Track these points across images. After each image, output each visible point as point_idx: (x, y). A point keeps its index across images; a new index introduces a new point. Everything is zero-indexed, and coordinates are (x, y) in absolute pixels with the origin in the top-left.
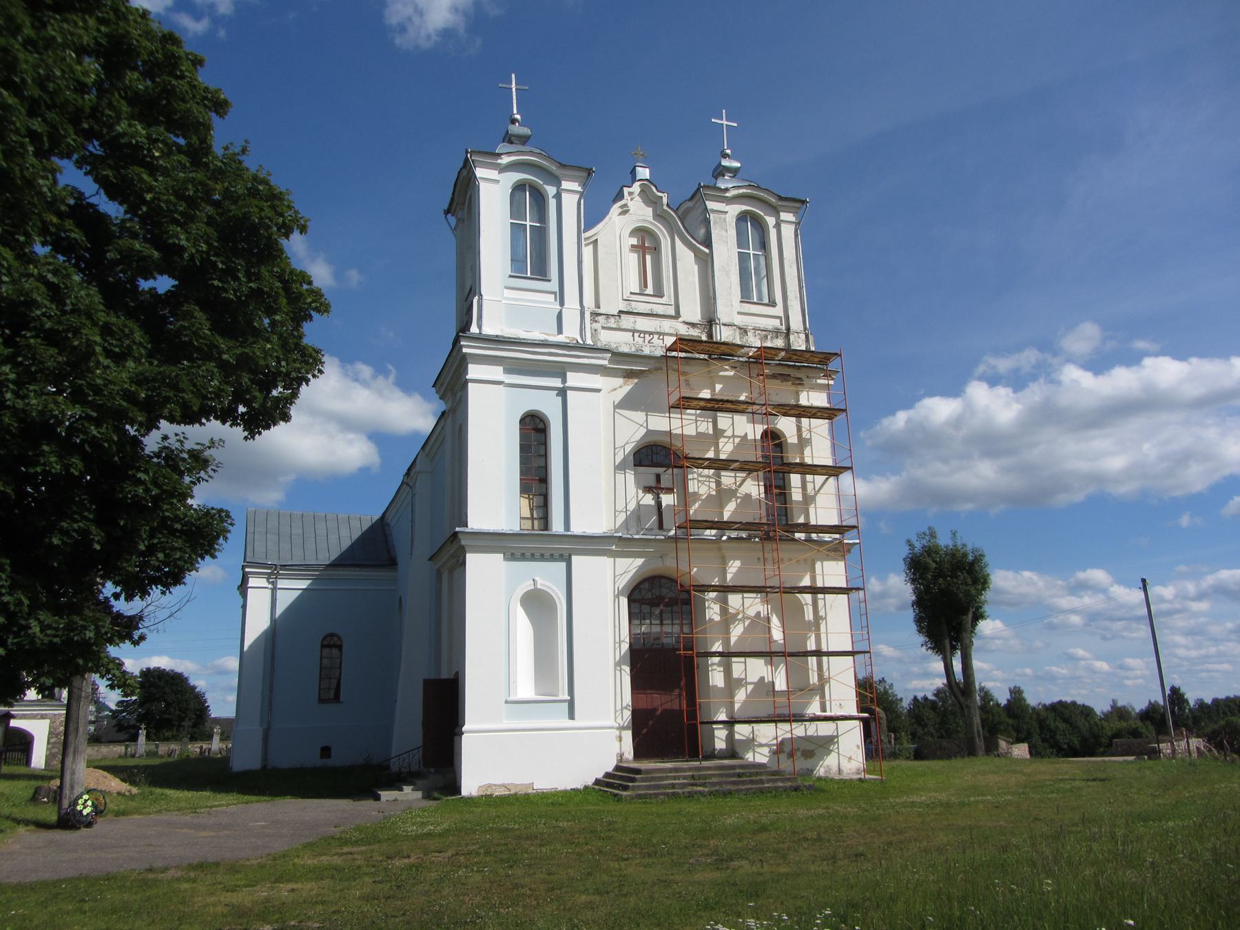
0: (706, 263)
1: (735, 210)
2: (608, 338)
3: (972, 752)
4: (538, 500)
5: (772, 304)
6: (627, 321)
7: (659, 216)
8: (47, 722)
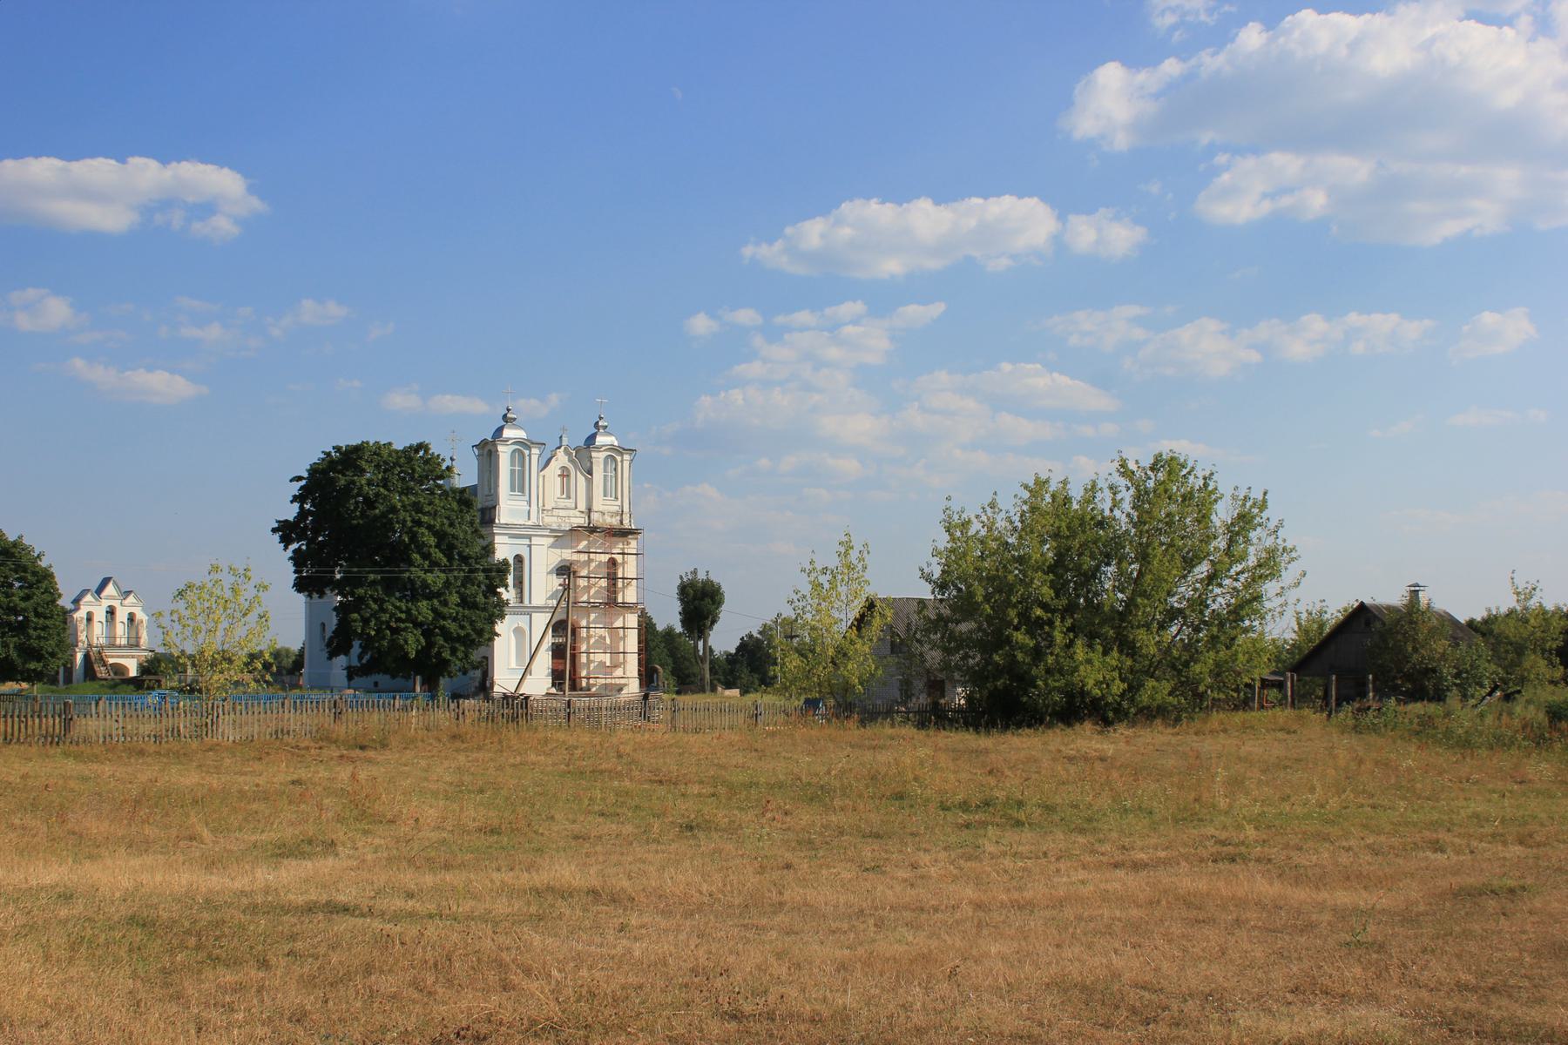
0: (590, 482)
1: (603, 455)
2: (548, 520)
3: (704, 692)
4: (519, 590)
5: (616, 498)
6: (556, 512)
7: (571, 461)
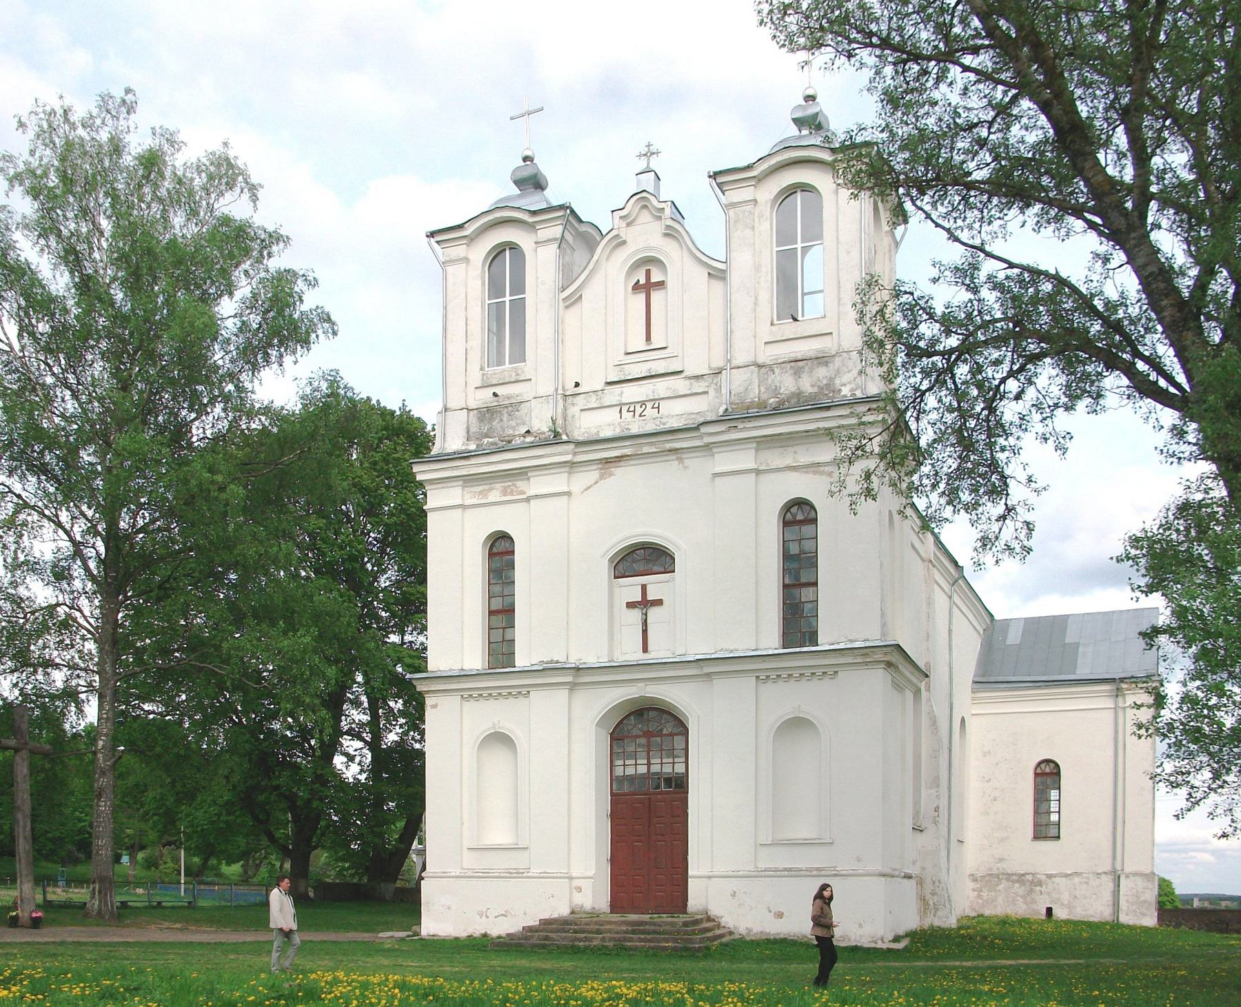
6: (613, 395)
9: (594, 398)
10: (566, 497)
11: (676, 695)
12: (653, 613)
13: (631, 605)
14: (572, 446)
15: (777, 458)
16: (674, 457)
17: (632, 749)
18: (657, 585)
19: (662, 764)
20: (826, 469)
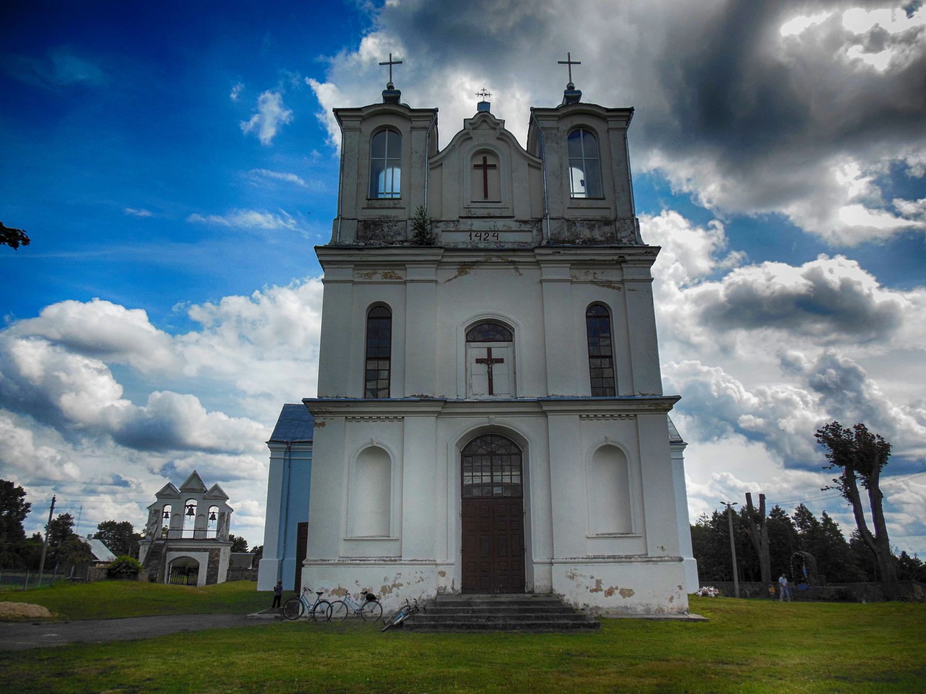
6: (466, 224)
8: (208, 553)
9: (452, 225)
10: (434, 284)
11: (521, 425)
12: (496, 367)
13: (479, 361)
14: (442, 251)
15: (581, 275)
16: (513, 267)
17: (479, 464)
18: (499, 349)
19: (502, 476)
20: (616, 285)
